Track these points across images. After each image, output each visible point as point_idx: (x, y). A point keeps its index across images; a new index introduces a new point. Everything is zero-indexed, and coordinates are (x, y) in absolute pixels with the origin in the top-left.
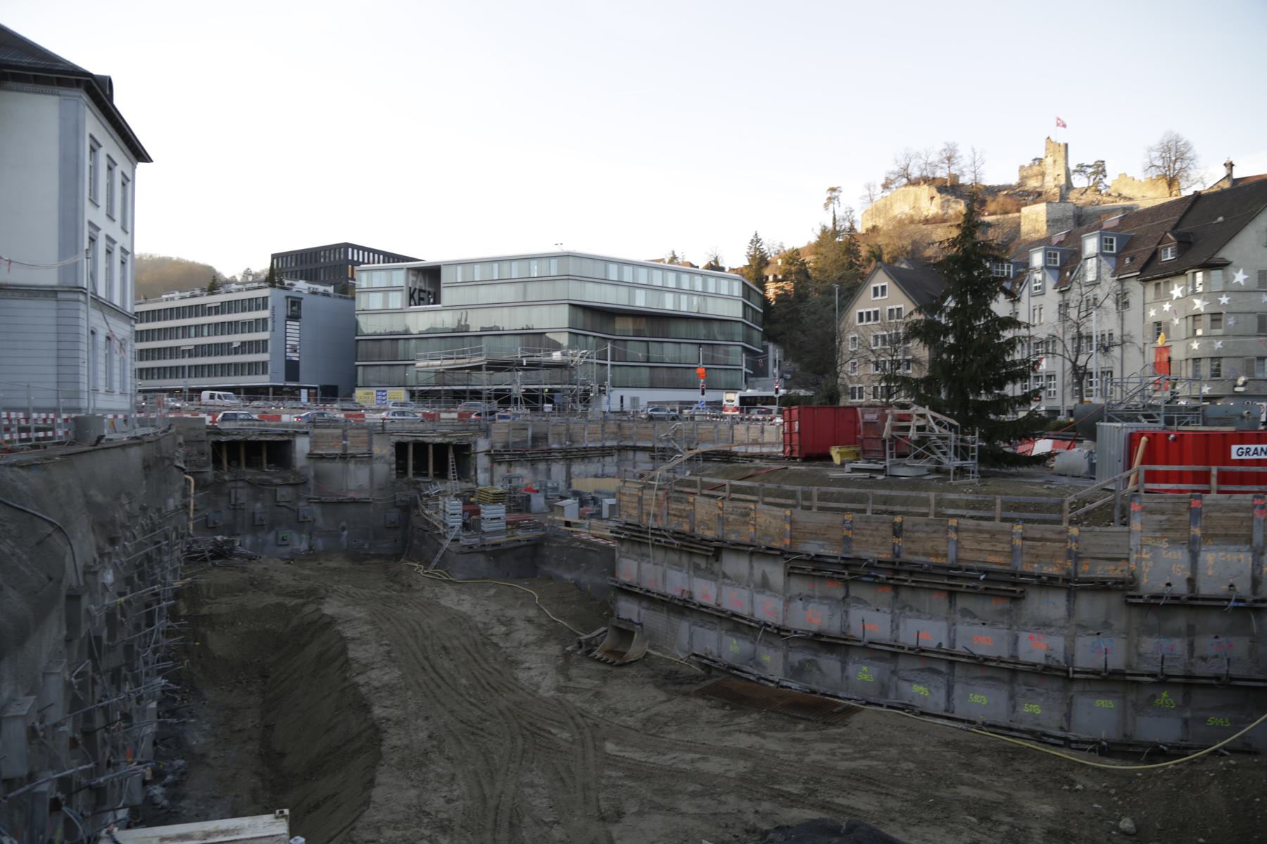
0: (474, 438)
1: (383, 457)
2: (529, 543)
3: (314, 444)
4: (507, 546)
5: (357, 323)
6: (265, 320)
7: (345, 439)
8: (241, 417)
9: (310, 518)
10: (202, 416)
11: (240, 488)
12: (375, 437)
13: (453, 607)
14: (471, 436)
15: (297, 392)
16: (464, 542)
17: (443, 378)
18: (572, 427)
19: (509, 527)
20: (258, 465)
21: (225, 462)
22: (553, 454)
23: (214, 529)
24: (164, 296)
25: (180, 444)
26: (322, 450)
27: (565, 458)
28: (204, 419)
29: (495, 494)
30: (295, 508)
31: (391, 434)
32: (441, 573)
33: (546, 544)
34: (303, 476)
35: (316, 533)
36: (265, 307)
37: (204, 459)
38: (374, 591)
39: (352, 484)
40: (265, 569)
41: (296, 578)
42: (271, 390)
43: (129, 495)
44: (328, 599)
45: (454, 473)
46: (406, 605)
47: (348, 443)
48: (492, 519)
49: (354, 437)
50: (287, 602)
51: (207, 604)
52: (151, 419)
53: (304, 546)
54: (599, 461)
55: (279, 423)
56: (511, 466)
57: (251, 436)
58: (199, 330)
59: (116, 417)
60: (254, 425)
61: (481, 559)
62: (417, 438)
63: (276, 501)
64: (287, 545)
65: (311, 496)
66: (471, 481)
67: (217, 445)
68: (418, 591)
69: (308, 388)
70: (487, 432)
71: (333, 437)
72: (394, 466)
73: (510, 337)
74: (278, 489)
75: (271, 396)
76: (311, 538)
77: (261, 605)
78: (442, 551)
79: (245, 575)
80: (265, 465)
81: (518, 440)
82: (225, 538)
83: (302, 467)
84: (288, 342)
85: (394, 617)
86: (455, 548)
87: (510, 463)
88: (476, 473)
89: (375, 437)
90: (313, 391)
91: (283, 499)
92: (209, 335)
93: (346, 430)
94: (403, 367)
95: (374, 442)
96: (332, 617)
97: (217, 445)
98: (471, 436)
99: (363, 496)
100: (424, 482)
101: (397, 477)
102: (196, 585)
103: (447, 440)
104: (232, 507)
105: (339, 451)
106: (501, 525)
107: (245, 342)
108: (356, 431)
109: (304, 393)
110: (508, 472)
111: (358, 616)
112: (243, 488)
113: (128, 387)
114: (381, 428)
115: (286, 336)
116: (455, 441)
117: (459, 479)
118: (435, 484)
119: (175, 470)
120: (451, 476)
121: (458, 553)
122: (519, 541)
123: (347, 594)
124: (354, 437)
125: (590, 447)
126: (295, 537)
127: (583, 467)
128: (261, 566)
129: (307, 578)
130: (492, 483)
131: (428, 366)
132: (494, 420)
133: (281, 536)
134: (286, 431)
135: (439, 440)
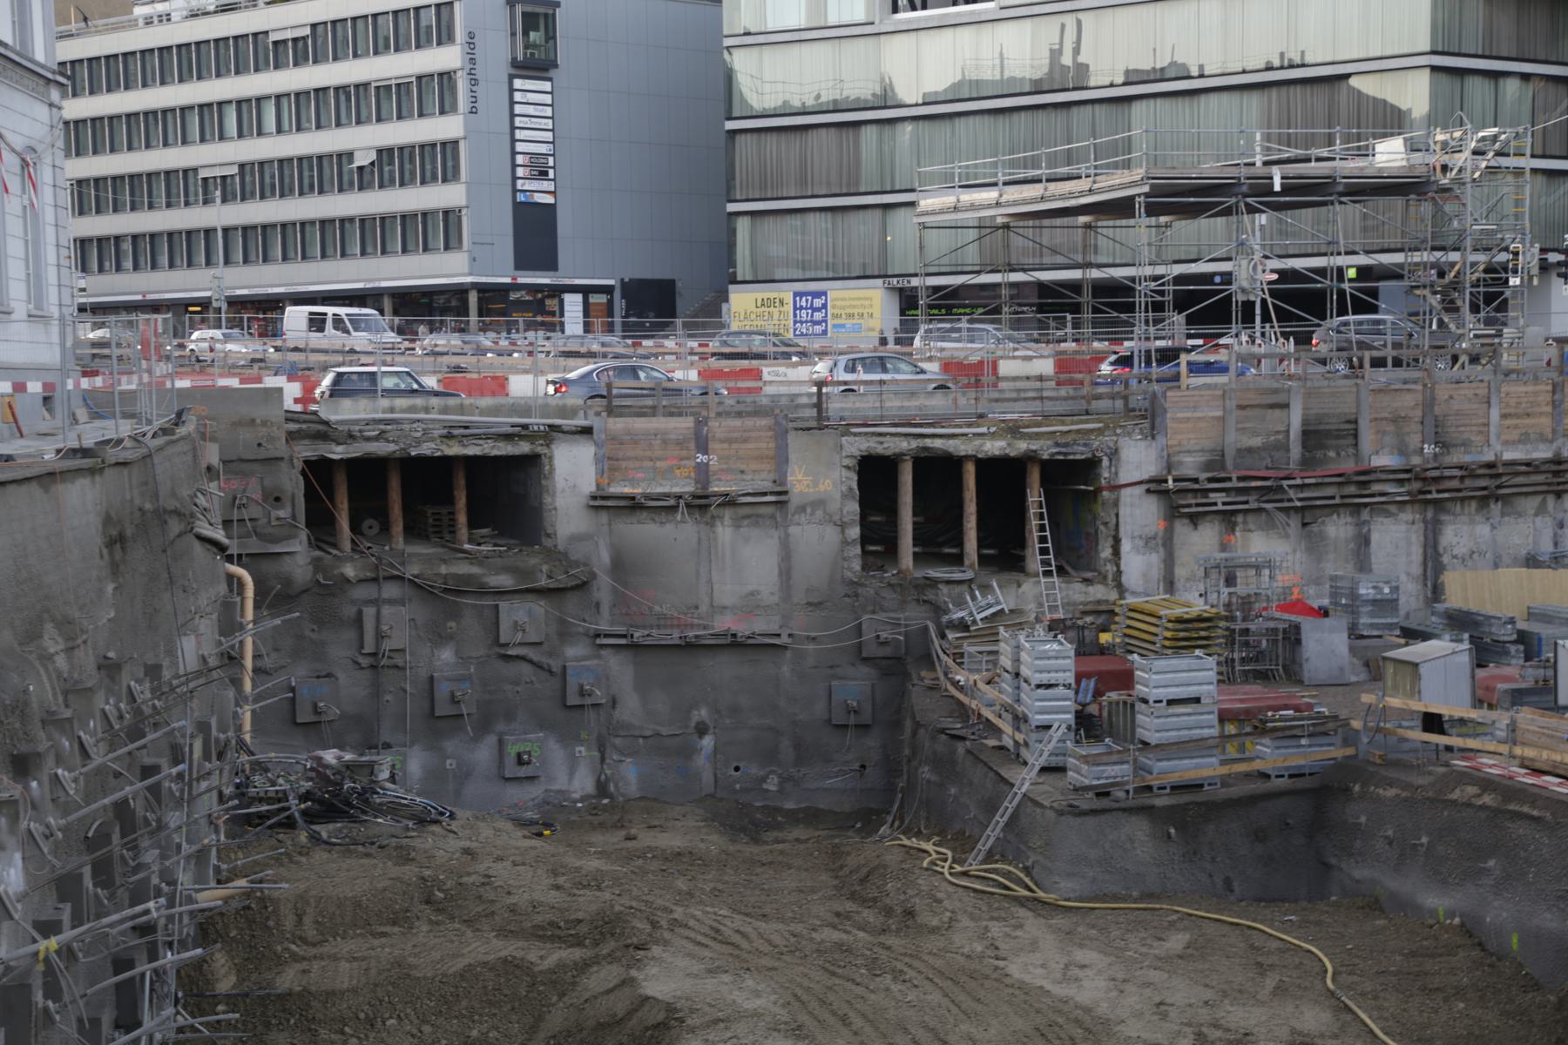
0: (1108, 440)
1: (820, 503)
2: (1300, 784)
3: (608, 464)
4: (1223, 793)
5: (729, 76)
6: (446, 77)
7: (703, 447)
8: (388, 383)
9: (599, 695)
10: (271, 382)
11: (391, 602)
12: (795, 441)
13: (1048, 987)
14: (1100, 432)
15: (552, 304)
16: (1081, 774)
17: (1007, 246)
18: (1442, 393)
19: (1231, 729)
20: (441, 532)
21: (344, 523)
22: (1376, 488)
23: (314, 729)
24: (139, 11)
25: (209, 468)
26: (633, 482)
27: (1418, 500)
28: (280, 390)
29: (1179, 620)
30: (556, 665)
31: (846, 429)
32: (1007, 875)
33: (1357, 788)
34: (577, 564)
35: (618, 741)
36: (445, 36)
37: (282, 513)
38: (798, 928)
39: (727, 592)
40: (467, 851)
41: (561, 880)
42: (473, 298)
43: (66, 626)
44: (656, 950)
45: (1044, 551)
46: (897, 975)
47: (714, 461)
48: (1171, 702)
49: (730, 441)
50: (532, 956)
51: (296, 958)
52: (122, 393)
53: (582, 783)
54: (1541, 510)
55: (500, 400)
56: (1232, 527)
57: (418, 442)
58: (249, 113)
59: (20, 387)
60: (427, 410)
61: (1138, 830)
62: (928, 442)
63: (497, 642)
64: (531, 779)
65: (604, 627)
66: (1103, 579)
67: (319, 472)
68: (934, 930)
69: (586, 291)
70: (1150, 419)
71: (665, 442)
72: (855, 532)
73: (1225, 96)
74: (504, 605)
75: (473, 318)
76: (603, 760)
77: (460, 964)
78: (1009, 805)
79: (409, 872)
80: (463, 532)
81: (1256, 442)
82: (348, 757)
83: (575, 538)
84: (520, 147)
85: (864, 1016)
86: (1051, 792)
87: (1228, 518)
88: (1116, 552)
89: (795, 441)
90: (601, 299)
91: (519, 637)
92: (279, 131)
93: (705, 422)
94: (878, 213)
95: (792, 457)
96: (670, 1008)
97: (319, 472)
98: (1100, 432)
99: (760, 625)
100: (949, 582)
101: (865, 567)
102: (262, 899)
103: (1022, 446)
104: (365, 662)
105: (686, 487)
106: (1204, 724)
107: (390, 150)
108: (737, 423)
109: (573, 304)
110: (1224, 547)
111: (750, 1005)
112: (401, 602)
113: (52, 295)
114: (814, 412)
115: (513, 128)
116: (1046, 449)
117: (1061, 571)
118: (986, 588)
119: (197, 546)
120: (1034, 561)
121: (1061, 813)
122: (1266, 776)
123: (716, 934)
124: (730, 441)
125: (1513, 463)
126: (555, 751)
127: (1483, 530)
128: (454, 844)
129: (595, 882)
130: (1170, 584)
131: (956, 209)
132: (1176, 378)
133: (512, 750)
134: (525, 427)
135: (995, 447)
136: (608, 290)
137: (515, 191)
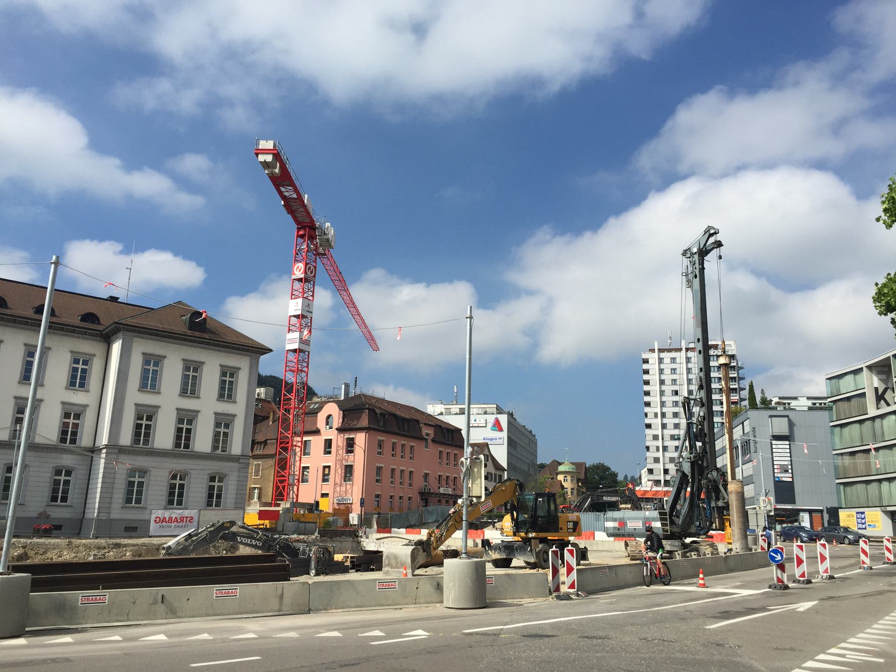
69: (810, 512)
84: (775, 463)
90: (816, 516)
136: (821, 511)
137: (774, 477)
